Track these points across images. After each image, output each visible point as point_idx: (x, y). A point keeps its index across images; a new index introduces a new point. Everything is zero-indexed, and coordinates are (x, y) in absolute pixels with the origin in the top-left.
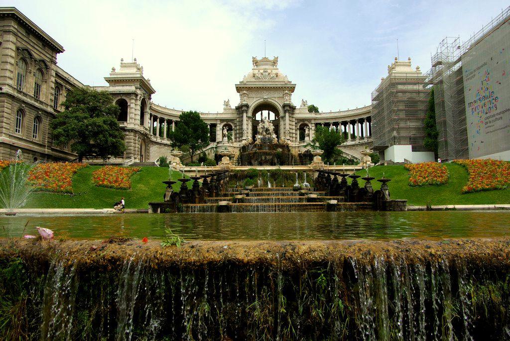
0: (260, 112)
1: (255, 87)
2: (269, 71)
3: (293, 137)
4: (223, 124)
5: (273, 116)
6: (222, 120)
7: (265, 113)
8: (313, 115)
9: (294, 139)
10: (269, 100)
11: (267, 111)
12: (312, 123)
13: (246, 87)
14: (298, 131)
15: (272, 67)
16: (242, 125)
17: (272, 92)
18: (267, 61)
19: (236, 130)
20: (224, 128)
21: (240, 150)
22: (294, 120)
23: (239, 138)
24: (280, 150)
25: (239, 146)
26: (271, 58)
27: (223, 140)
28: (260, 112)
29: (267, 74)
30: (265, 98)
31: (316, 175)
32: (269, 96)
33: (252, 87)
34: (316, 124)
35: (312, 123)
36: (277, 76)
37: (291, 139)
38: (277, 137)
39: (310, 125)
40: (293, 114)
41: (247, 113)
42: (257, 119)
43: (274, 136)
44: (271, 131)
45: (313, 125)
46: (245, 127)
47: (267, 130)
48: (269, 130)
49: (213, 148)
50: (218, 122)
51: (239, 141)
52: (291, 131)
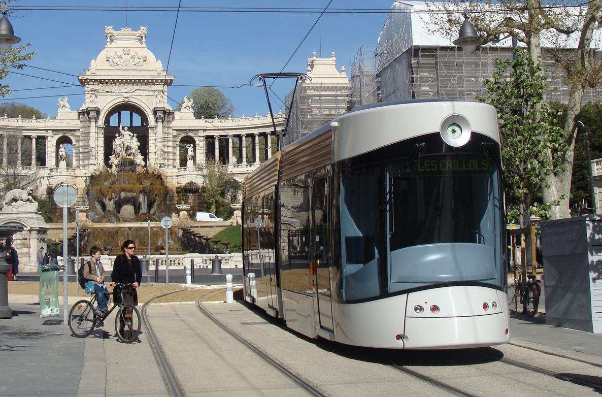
0: (117, 113)
3: (168, 159)
4: (57, 137)
5: (137, 121)
7: (125, 114)
8: (201, 123)
9: (171, 162)
10: (132, 100)
11: (128, 112)
13: (96, 80)
14: (178, 149)
15: (138, 44)
16: (88, 139)
19: (79, 147)
20: (61, 146)
21: (86, 181)
22: (171, 131)
23: (84, 160)
24: (147, 183)
25: (84, 175)
27: (57, 165)
28: (117, 113)
31: (181, 232)
34: (207, 137)
37: (166, 162)
38: (145, 160)
39: (196, 139)
40: (169, 122)
41: (96, 122)
42: (110, 125)
43: (139, 159)
44: (133, 151)
46: (92, 143)
47: (128, 148)
49: (43, 177)
50: (50, 133)
51: (84, 166)
52: (166, 150)
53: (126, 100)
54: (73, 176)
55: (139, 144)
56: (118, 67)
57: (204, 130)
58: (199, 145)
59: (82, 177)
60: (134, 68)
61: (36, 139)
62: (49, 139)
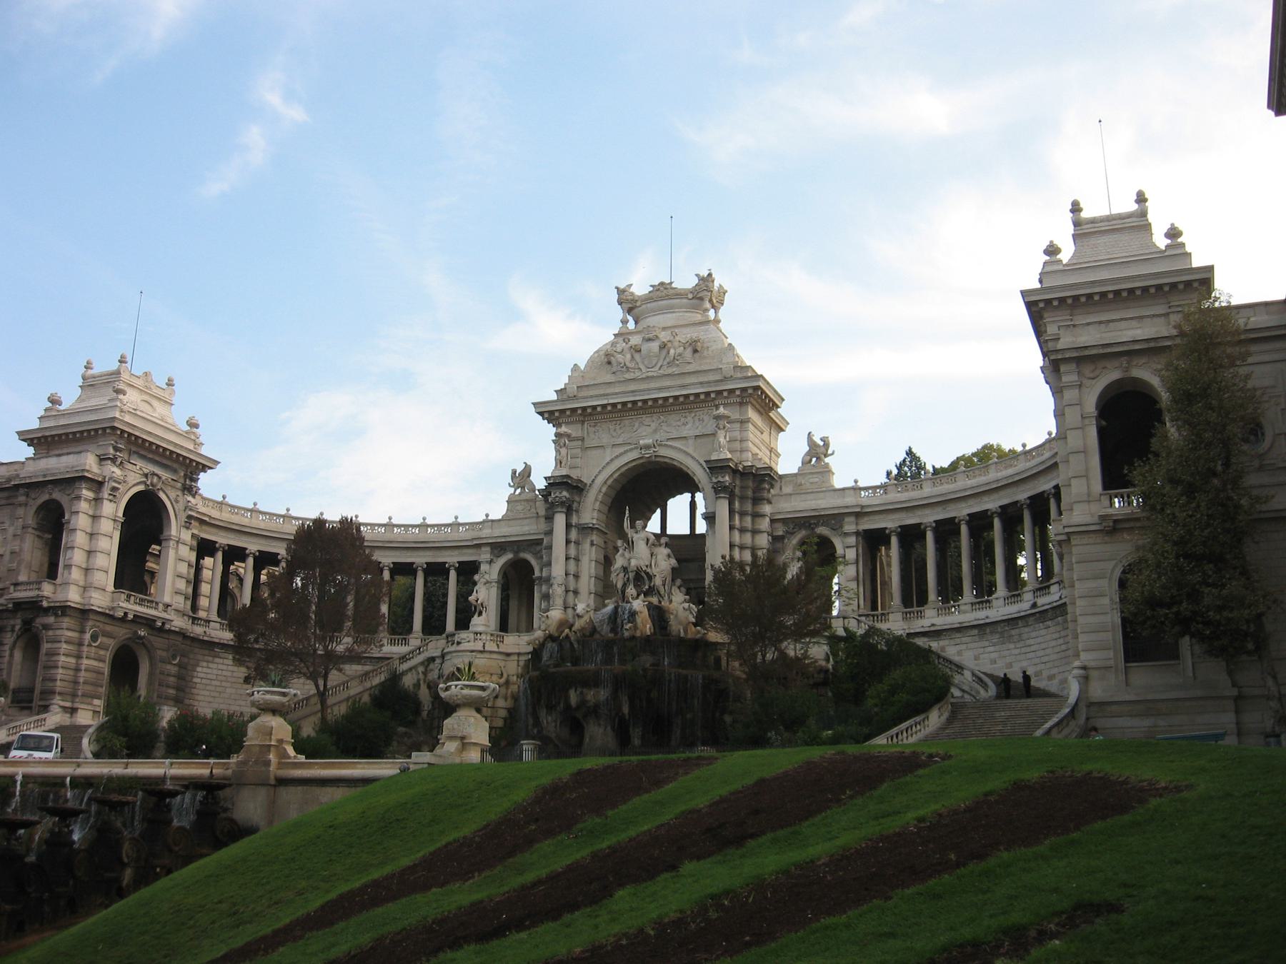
1: (604, 406)
2: (665, 337)
4: (501, 562)
6: (498, 547)
10: (663, 452)
12: (846, 534)
13: (574, 410)
17: (673, 419)
18: (668, 297)
26: (686, 282)
29: (655, 346)
30: (647, 447)
32: (661, 436)
33: (594, 407)
35: (846, 534)
36: (695, 351)
41: (569, 511)
42: (669, 532)
44: (658, 581)
45: (852, 540)
48: (650, 577)
50: (484, 555)
53: (648, 453)
54: (491, 652)
55: (673, 562)
56: (628, 376)
57: (858, 515)
58: (844, 557)
59: (519, 654)
60: (670, 371)
61: (456, 569)
62: (484, 567)
